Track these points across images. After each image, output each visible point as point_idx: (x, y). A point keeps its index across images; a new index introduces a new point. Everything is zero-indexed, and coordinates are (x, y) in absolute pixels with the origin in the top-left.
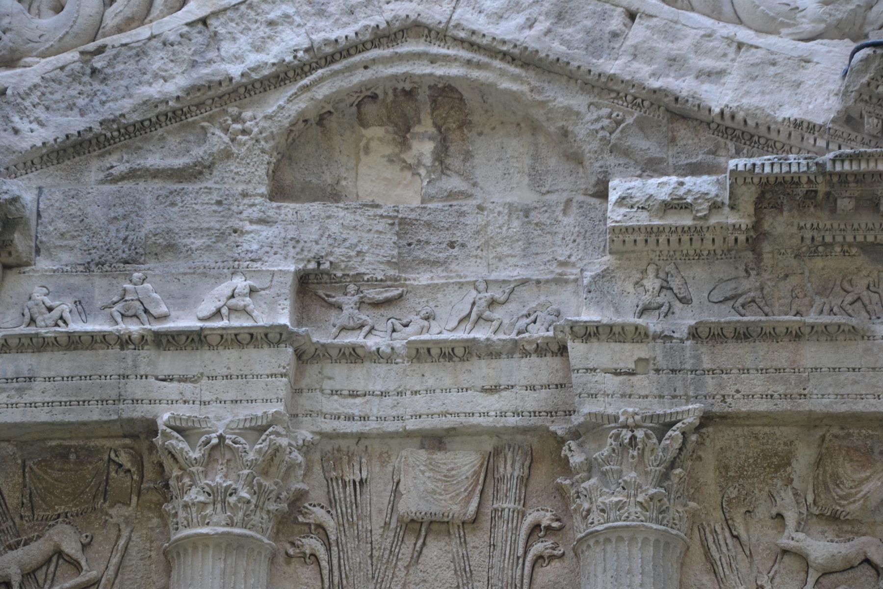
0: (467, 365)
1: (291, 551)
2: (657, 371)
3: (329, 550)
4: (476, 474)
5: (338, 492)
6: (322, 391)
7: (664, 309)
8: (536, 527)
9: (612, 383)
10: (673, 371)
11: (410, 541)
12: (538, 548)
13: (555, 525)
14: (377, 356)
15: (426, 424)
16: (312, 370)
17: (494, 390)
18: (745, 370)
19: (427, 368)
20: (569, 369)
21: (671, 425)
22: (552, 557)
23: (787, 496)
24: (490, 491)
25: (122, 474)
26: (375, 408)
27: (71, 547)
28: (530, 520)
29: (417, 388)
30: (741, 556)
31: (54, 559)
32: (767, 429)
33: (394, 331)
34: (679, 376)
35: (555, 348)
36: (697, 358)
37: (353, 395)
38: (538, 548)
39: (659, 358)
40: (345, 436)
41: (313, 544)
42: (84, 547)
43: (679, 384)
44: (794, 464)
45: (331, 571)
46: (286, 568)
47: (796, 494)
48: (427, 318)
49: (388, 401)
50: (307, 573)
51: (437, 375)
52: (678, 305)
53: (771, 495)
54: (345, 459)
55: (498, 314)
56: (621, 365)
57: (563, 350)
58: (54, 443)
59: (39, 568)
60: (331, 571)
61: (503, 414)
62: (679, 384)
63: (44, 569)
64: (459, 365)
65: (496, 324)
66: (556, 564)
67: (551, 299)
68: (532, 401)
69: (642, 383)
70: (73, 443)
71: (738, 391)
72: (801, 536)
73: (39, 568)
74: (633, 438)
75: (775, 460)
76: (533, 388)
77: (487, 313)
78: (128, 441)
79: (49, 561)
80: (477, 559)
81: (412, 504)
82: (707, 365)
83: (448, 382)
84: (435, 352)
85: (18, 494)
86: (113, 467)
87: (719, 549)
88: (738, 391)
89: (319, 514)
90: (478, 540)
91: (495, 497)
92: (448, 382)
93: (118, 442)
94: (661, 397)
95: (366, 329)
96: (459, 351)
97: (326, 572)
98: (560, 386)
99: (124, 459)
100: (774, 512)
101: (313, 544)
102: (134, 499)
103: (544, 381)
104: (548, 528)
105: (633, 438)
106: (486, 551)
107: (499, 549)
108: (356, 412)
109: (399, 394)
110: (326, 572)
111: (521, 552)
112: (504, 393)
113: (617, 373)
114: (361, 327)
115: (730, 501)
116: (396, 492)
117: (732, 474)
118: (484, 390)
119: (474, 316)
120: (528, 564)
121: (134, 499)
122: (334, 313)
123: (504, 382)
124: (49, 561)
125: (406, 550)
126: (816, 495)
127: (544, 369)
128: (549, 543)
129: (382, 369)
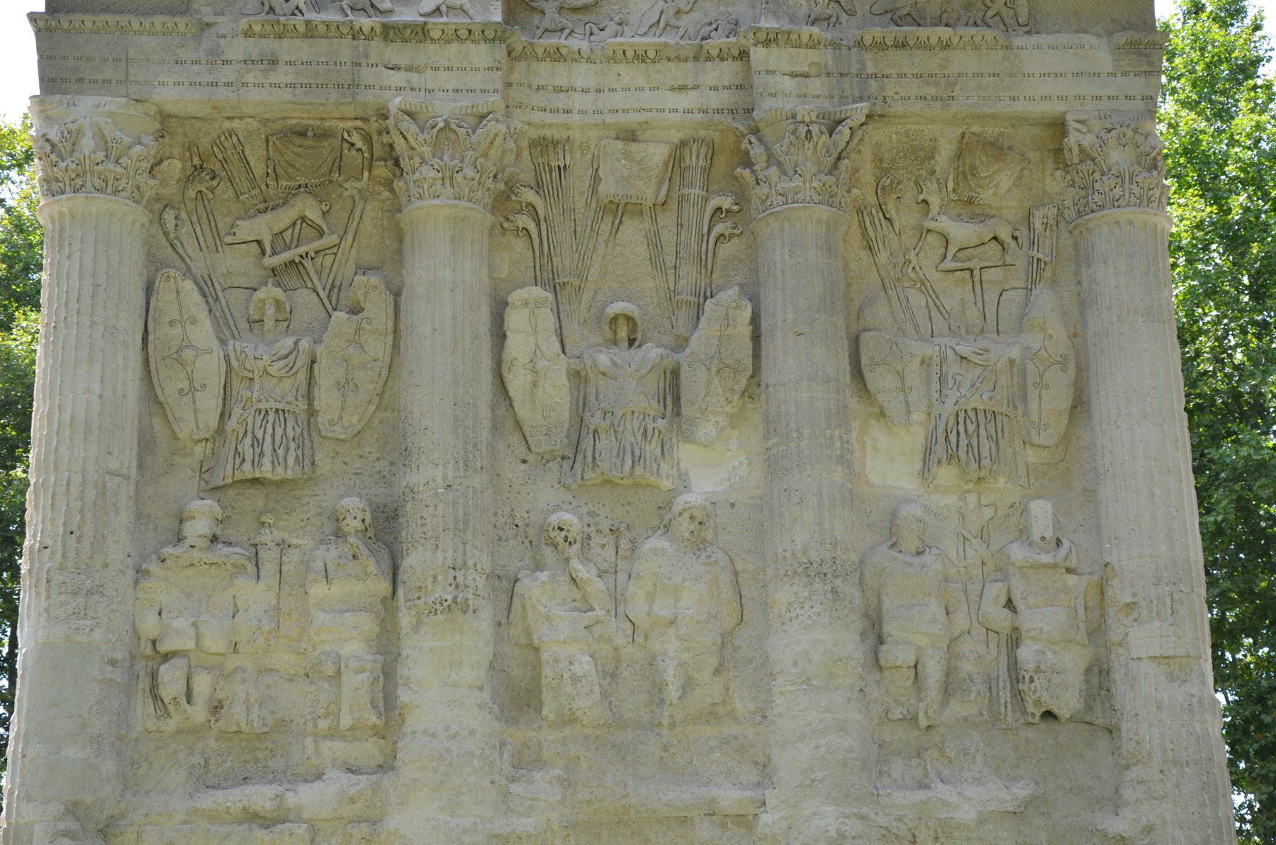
0: (658, 66)
1: (506, 225)
2: (828, 74)
3: (538, 225)
4: (666, 163)
5: (546, 178)
6: (530, 86)
7: (833, 20)
8: (719, 209)
9: (789, 84)
10: (842, 75)
11: (608, 220)
12: (719, 228)
13: (735, 208)
14: (578, 57)
15: (621, 118)
16: (521, 67)
17: (683, 88)
18: (902, 76)
19: (621, 68)
20: (748, 69)
21: (840, 122)
22: (732, 236)
23: (932, 186)
24: (677, 179)
25: (354, 152)
26: (577, 101)
27: (313, 214)
28: (714, 202)
29: (613, 86)
30: (892, 235)
31: (299, 222)
32: (916, 127)
33: (591, 34)
34: (846, 79)
35: (736, 53)
36: (863, 63)
37: (558, 90)
38: (719, 228)
39: (830, 63)
40: (550, 125)
41: (524, 221)
42: (324, 214)
43: (846, 86)
44: (937, 157)
45: (541, 243)
46: (501, 239)
47: (939, 183)
48: (621, 24)
49: (589, 97)
50: (520, 245)
51: (629, 74)
52: (844, 17)
53: (917, 184)
54: (551, 148)
55: (685, 21)
56: (798, 69)
57: (743, 55)
58: (294, 122)
59: (286, 230)
60: (541, 243)
61: (690, 111)
62: (846, 86)
63: (290, 231)
64: (651, 66)
65: (682, 30)
66: (735, 241)
67: (730, 9)
68: (715, 100)
69: (816, 86)
70: (310, 122)
71: (896, 93)
72: (943, 218)
73: (286, 230)
74: (809, 132)
75: (921, 154)
76: (716, 89)
77: (673, 22)
78: (359, 123)
79: (294, 224)
80: (668, 236)
81: (608, 188)
82: (870, 69)
83: (641, 82)
84: (630, 54)
85: (263, 165)
86: (346, 146)
87: (875, 230)
88: (896, 93)
89: (529, 196)
90: (667, 221)
91: (682, 184)
92: (641, 82)
93: (350, 124)
94: (832, 97)
95: (567, 32)
96: (651, 54)
97: (536, 244)
98: (740, 87)
99: (356, 138)
100: (921, 197)
101: (524, 221)
102: (366, 174)
103: (726, 83)
104: (728, 211)
105: (809, 132)
106: (674, 229)
107: (685, 227)
108: (561, 106)
109: (598, 91)
110: (536, 244)
111: (705, 231)
112: (691, 93)
113: (794, 75)
114: (562, 30)
115: (884, 188)
116: (596, 179)
117: (885, 165)
118: (672, 89)
119: (662, 24)
120: (712, 241)
121: (366, 174)
122: (537, 17)
123: (690, 83)
124: (294, 224)
125: (606, 227)
126: (956, 184)
127: (727, 72)
128: (729, 224)
129: (582, 67)
